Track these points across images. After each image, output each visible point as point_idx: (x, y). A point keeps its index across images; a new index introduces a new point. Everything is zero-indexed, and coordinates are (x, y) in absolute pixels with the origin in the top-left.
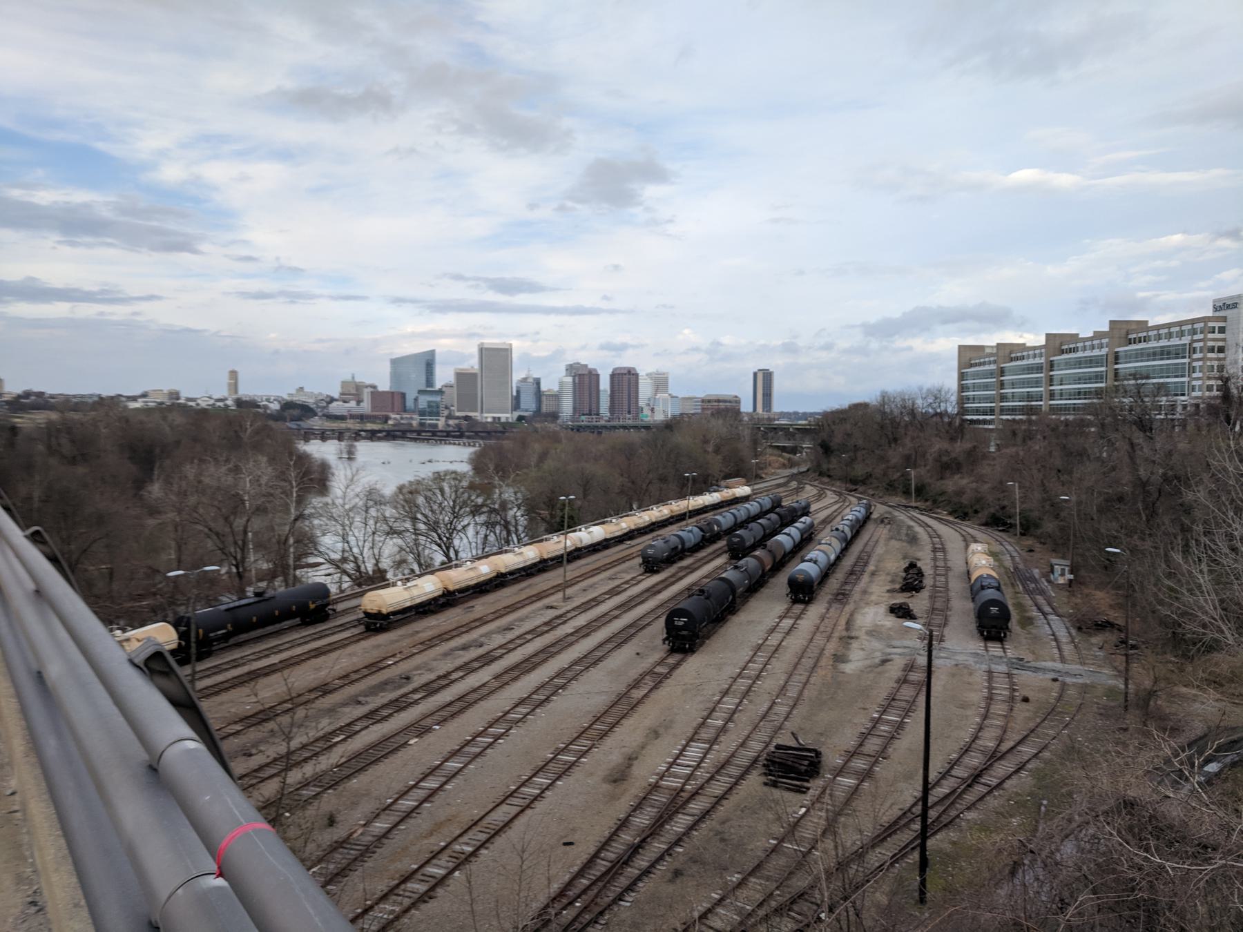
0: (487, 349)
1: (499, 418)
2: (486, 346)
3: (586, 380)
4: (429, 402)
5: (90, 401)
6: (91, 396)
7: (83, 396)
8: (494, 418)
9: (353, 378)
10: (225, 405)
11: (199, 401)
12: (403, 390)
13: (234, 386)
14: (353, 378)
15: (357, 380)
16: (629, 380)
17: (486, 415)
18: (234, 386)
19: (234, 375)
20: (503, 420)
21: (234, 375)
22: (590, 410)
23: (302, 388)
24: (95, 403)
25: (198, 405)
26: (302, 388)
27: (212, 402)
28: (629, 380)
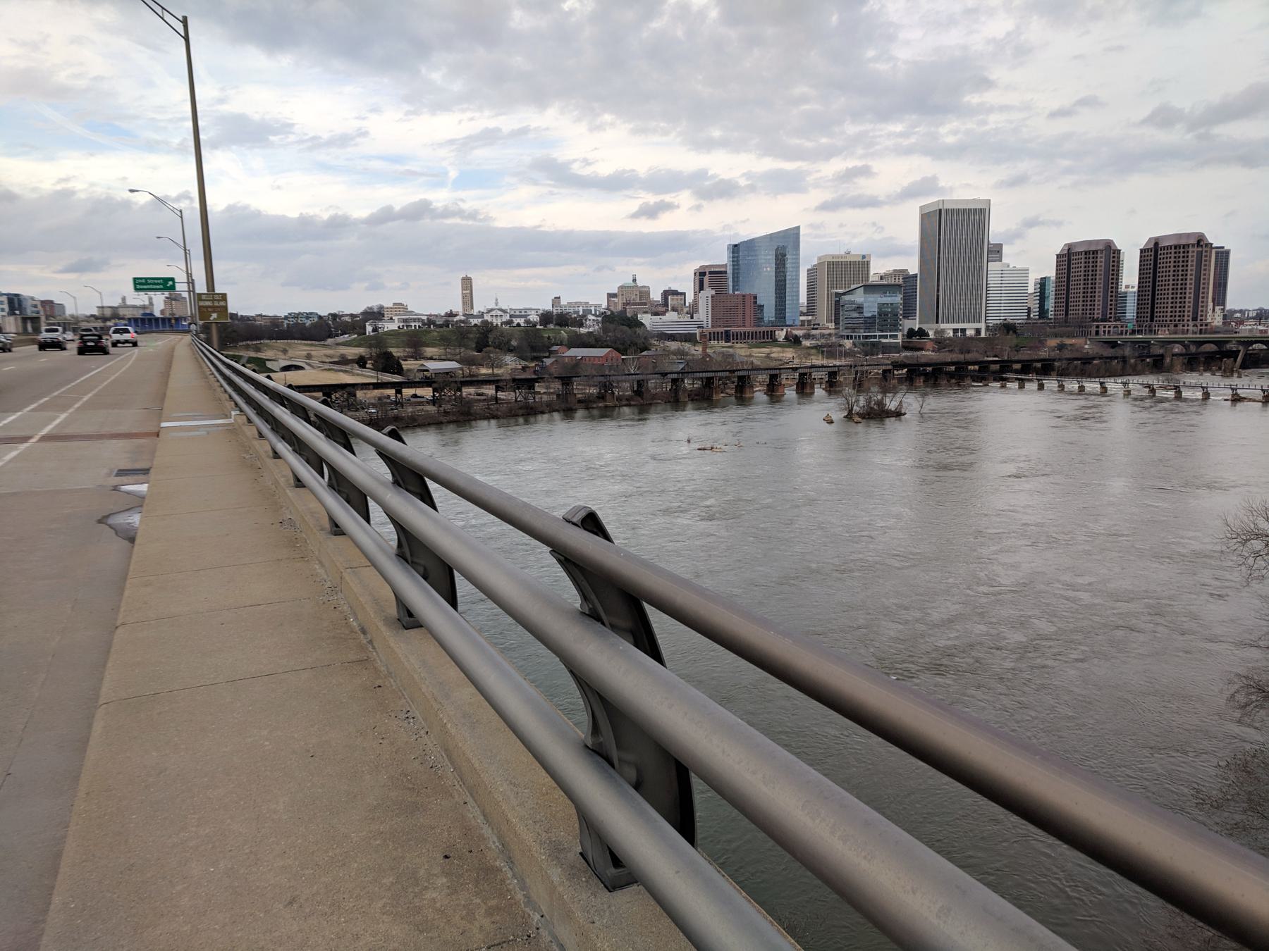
0: (948, 211)
1: (963, 331)
2: (947, 206)
3: (1101, 260)
4: (881, 306)
5: (308, 323)
6: (308, 316)
7: (297, 316)
8: (955, 331)
9: (634, 280)
10: (527, 322)
11: (487, 317)
12: (754, 292)
13: (468, 298)
14: (634, 280)
15: (639, 283)
16: (1200, 254)
17: (943, 326)
18: (468, 298)
19: (467, 283)
20: (970, 333)
21: (467, 283)
22: (1104, 314)
23: (559, 298)
24: (314, 326)
25: (486, 323)
26: (559, 298)
27: (506, 318)
28: (1200, 254)
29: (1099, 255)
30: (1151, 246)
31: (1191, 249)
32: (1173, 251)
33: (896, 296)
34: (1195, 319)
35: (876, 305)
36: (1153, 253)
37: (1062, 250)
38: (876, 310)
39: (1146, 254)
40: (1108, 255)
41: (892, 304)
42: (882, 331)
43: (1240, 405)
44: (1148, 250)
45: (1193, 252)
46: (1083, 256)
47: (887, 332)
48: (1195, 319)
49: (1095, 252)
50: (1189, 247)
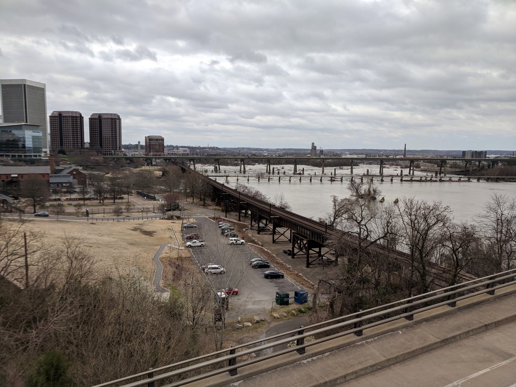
2: (27, 83)
4: (34, 138)
29: (78, 119)
30: (97, 117)
31: (117, 121)
32: (110, 120)
33: (40, 132)
34: (120, 149)
35: (31, 137)
36: (98, 120)
37: (53, 114)
38: (31, 140)
39: (92, 120)
40: (77, 119)
41: (38, 137)
42: (34, 153)
43: (333, 182)
44: (55, 117)
45: (118, 121)
46: (70, 118)
47: (37, 153)
48: (120, 149)
49: (77, 117)
50: (77, 118)
